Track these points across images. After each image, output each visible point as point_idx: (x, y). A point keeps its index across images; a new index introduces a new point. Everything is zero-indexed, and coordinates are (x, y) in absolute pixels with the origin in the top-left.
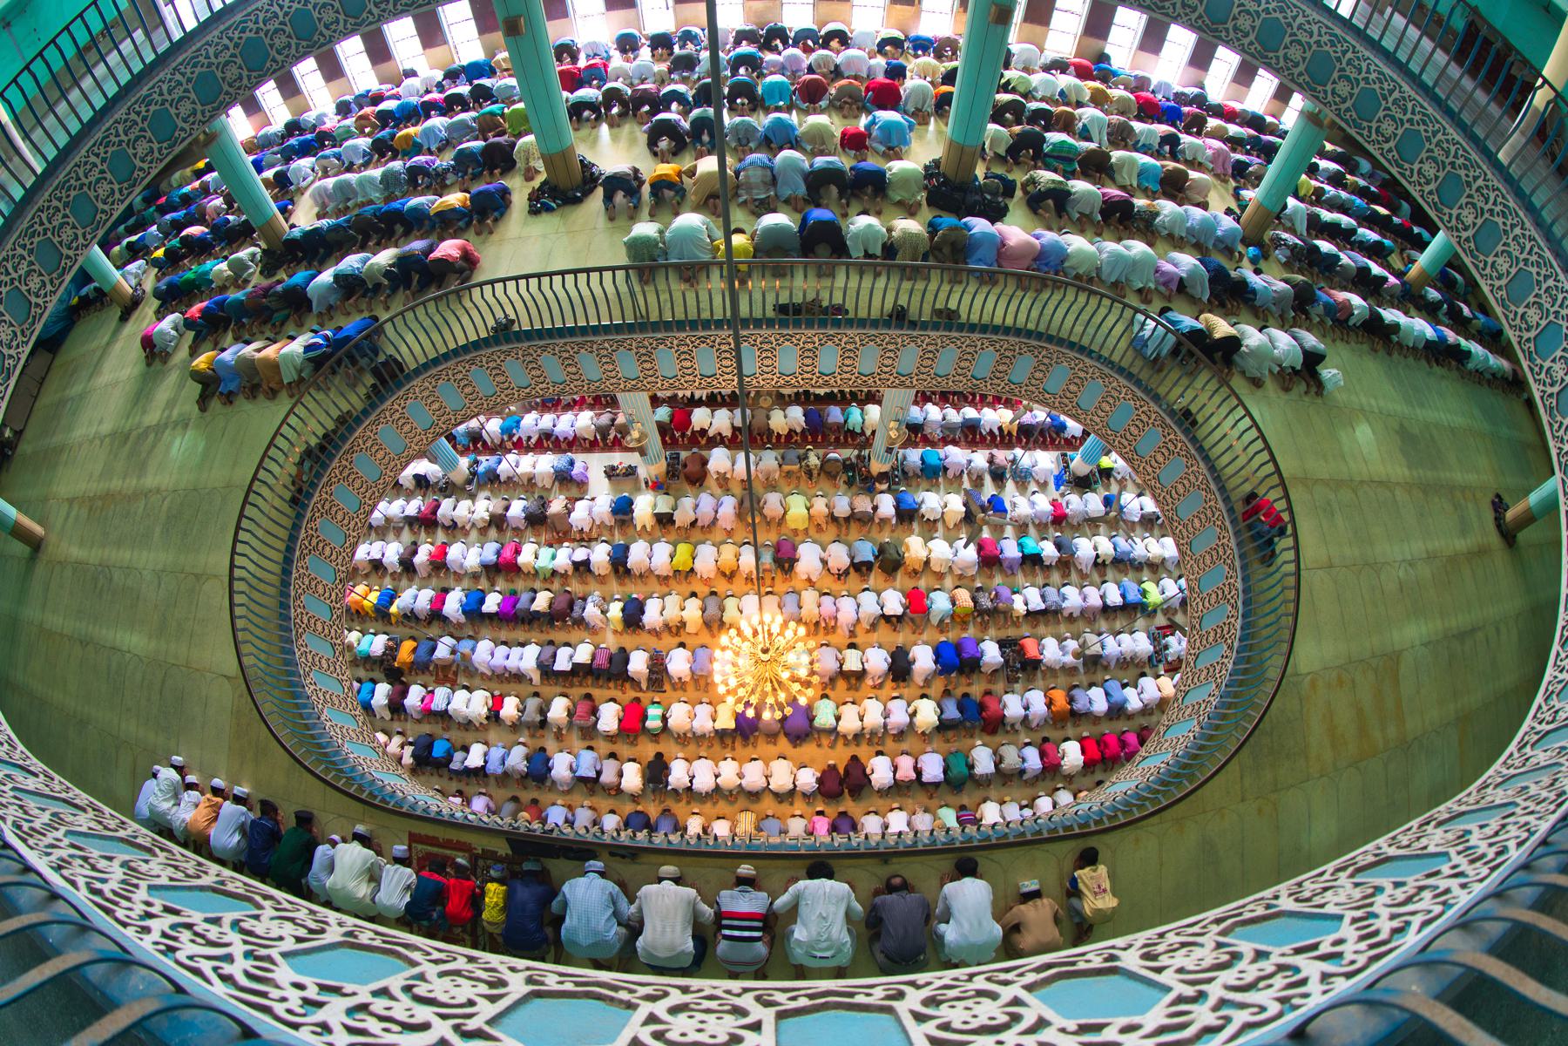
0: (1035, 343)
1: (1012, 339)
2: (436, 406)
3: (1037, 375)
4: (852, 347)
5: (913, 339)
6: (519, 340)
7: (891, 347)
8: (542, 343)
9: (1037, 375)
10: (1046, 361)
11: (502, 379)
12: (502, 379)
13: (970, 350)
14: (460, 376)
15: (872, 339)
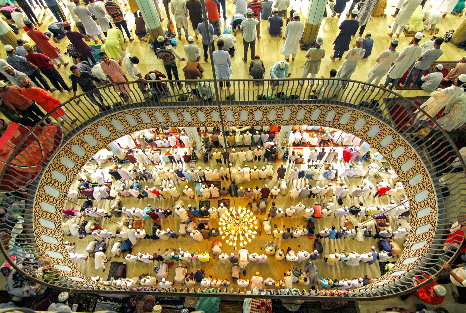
0: (335, 106)
1: (326, 105)
2: (111, 129)
3: (336, 118)
4: (266, 111)
5: (288, 108)
6: (145, 106)
7: (280, 111)
8: (155, 107)
9: (337, 118)
10: (340, 112)
11: (140, 120)
12: (140, 120)
13: (310, 110)
14: (122, 118)
15: (273, 108)
